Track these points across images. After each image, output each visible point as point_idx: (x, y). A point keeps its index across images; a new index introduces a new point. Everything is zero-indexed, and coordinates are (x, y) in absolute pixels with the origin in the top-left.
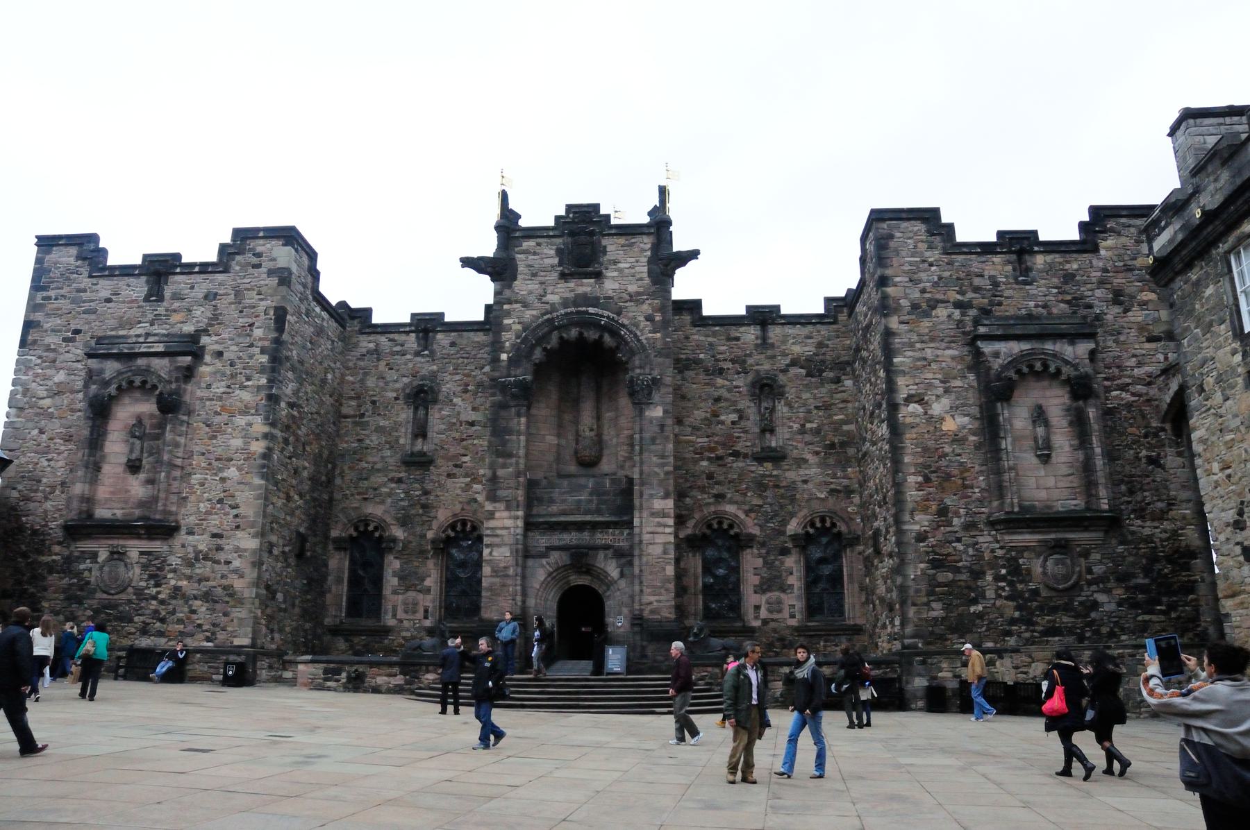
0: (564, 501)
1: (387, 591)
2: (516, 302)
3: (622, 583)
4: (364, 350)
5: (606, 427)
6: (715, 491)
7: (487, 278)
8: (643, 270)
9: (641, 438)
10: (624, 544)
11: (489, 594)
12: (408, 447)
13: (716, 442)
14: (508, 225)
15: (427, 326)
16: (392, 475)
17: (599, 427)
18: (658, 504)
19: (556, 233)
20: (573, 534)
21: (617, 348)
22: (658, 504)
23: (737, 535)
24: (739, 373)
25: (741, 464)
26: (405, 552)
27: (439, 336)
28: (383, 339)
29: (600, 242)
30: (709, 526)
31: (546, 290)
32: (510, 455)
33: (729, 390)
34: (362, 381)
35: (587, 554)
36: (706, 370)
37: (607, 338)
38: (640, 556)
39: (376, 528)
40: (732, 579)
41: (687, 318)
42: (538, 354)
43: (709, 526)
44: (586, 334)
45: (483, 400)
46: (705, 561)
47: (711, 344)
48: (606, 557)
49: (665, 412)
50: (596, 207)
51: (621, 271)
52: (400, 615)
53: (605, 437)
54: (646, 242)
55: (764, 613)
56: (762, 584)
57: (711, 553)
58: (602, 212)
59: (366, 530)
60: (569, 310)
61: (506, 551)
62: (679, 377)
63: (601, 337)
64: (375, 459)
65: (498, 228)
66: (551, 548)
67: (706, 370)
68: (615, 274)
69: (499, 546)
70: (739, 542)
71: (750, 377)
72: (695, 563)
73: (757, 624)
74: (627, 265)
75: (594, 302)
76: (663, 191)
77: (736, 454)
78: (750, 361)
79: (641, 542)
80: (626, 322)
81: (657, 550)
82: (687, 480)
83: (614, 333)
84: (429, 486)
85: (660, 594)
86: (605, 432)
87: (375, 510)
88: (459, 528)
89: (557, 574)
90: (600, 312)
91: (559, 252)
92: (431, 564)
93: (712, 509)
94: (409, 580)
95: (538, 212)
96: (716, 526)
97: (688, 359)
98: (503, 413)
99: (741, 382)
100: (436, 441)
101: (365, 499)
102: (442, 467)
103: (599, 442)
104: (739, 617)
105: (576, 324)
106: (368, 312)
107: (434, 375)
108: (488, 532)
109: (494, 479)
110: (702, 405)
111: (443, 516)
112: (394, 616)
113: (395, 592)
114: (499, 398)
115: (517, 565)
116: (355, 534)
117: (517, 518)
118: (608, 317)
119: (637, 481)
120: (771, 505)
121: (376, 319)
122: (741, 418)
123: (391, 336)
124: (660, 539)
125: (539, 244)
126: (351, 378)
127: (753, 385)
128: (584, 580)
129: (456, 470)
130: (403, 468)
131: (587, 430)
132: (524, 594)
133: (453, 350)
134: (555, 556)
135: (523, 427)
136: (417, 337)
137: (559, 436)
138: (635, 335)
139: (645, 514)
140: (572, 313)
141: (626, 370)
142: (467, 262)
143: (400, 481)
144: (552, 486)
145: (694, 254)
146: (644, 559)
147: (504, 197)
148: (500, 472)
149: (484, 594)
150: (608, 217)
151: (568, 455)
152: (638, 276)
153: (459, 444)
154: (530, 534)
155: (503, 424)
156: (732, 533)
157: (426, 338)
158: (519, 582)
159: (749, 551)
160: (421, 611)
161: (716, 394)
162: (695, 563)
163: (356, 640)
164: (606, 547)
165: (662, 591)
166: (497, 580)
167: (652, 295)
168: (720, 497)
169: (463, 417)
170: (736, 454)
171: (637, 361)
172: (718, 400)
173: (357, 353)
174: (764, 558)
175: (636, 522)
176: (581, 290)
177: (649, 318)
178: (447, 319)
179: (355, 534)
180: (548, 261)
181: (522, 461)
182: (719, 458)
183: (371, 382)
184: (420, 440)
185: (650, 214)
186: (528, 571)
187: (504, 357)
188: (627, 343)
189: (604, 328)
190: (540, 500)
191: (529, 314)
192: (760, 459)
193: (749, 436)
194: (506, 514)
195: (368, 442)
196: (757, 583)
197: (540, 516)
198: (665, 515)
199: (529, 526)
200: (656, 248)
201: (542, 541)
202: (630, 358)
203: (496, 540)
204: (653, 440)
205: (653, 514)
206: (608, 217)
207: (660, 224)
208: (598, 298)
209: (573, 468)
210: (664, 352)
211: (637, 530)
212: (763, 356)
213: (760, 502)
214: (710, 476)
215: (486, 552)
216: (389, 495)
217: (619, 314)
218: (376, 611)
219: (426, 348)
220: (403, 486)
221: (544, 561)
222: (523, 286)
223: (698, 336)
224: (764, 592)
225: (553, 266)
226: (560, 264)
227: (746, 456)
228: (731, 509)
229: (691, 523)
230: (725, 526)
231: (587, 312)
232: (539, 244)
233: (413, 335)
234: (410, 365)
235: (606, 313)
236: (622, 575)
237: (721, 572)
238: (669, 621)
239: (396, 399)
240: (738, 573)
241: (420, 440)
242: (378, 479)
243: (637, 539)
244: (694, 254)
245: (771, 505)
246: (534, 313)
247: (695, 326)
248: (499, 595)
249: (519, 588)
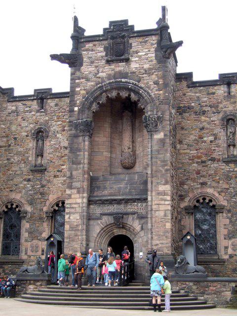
0: (111, 188)
1: (22, 240)
2: (83, 78)
3: (142, 234)
4: (10, 111)
5: (138, 146)
6: (201, 181)
7: (67, 65)
8: (152, 55)
9: (151, 151)
10: (143, 212)
11: (68, 240)
12: (33, 162)
13: (202, 153)
14: (79, 37)
15: (42, 96)
17: (133, 146)
18: (162, 188)
19: (104, 38)
20: (115, 206)
21: (139, 100)
22: (162, 188)
23: (214, 206)
24: (214, 113)
25: (215, 165)
26: (31, 220)
27: (49, 101)
28: (20, 104)
29: (128, 41)
30: (198, 201)
31: (99, 69)
32: (80, 163)
33: (209, 123)
34: (9, 128)
35: (123, 217)
36: (196, 113)
38: (151, 218)
39: (17, 206)
40: (212, 231)
41: (184, 83)
42: (95, 107)
43: (198, 201)
44: (121, 94)
46: (196, 220)
47: (198, 97)
48: (133, 219)
49: (165, 135)
50: (126, 22)
51: (140, 57)
52: (29, 253)
53: (137, 152)
54: (154, 39)
55: (230, 251)
56: (229, 234)
57: (198, 216)
58: (130, 24)
59: (12, 207)
60: (111, 81)
61: (77, 216)
62: (180, 117)
63: (130, 95)
64: (17, 169)
65: (73, 37)
66: (102, 214)
67: (196, 113)
68: (137, 59)
69: (74, 213)
70: (214, 210)
71: (221, 115)
72: (189, 222)
73: (226, 257)
74: (144, 53)
75: (125, 75)
76: (164, 9)
77: (213, 160)
78: (221, 106)
79: (152, 210)
80: (143, 86)
81: (162, 214)
82: (184, 175)
83: (137, 93)
84: (44, 183)
85: (163, 240)
86: (137, 149)
87: (16, 197)
88: (60, 205)
89: (106, 229)
90: (128, 81)
91: (106, 49)
92: (45, 224)
93: (200, 191)
94: (34, 234)
95: (94, 27)
96: (201, 201)
97: (185, 107)
98: (75, 140)
99: (216, 118)
100: (48, 158)
101: (11, 191)
102: (51, 171)
103: (134, 154)
104: (216, 253)
105: (115, 89)
106: (11, 90)
107: (47, 122)
108: (68, 206)
109: (71, 177)
110: (193, 132)
111: (52, 198)
112: (26, 254)
113: (26, 241)
114: (73, 132)
115: (83, 224)
116: (6, 210)
117: (83, 198)
118: (133, 84)
119: (149, 175)
120: (234, 188)
121: (16, 94)
122: (215, 139)
123: (24, 102)
124: (162, 208)
125: (95, 45)
126: (3, 126)
127: (222, 119)
128: (122, 232)
129: (58, 174)
131: (126, 148)
132: (88, 240)
133: (56, 108)
134: (105, 218)
135: (86, 148)
136: (37, 103)
137: (111, 152)
138: (148, 93)
139: (154, 193)
140: (113, 82)
141: (144, 113)
142: (54, 57)
143: (29, 180)
144: (105, 180)
146: (154, 220)
147: (76, 20)
148: (74, 173)
150: (132, 27)
151: (117, 163)
152: (149, 59)
153: (60, 159)
154: (92, 206)
155: (76, 146)
156: (211, 204)
157: (42, 103)
158: (84, 233)
159: (221, 214)
160: (40, 251)
161: (201, 126)
162: (189, 222)
163: (6, 267)
164: (133, 213)
165: (164, 237)
166: (73, 232)
167: (158, 70)
168: (203, 184)
169: (62, 144)
170: (213, 160)
171: (149, 108)
172: (203, 129)
173: (6, 112)
174: (230, 219)
175: (149, 198)
176: (117, 69)
177: (156, 83)
178: (53, 92)
179: (6, 210)
180: (99, 54)
181: (86, 166)
182: (203, 162)
183: (14, 128)
184: (40, 158)
185: (157, 23)
186: (91, 227)
187: (76, 109)
188: (143, 98)
189: (130, 90)
190: (99, 188)
191: (90, 84)
192: (227, 162)
193: (221, 149)
194: (78, 196)
195: (12, 160)
196: (226, 233)
197: (97, 196)
198: (165, 194)
199: (90, 202)
200: (159, 43)
201: (97, 210)
202: (145, 106)
203: (72, 210)
204: (158, 151)
205: (159, 194)
206: (132, 27)
207: (162, 29)
208: (127, 73)
209: (120, 170)
210: (166, 101)
211: (149, 203)
212: (228, 103)
213: (228, 187)
214: (198, 173)
215: (67, 217)
216: (24, 188)
217: (139, 82)
218: (17, 251)
219: (42, 108)
220: (31, 183)
221: (99, 222)
222: (86, 69)
223: (191, 93)
224: (230, 239)
225: (102, 57)
226: (106, 55)
227: (219, 160)
228: (210, 191)
229: (187, 199)
230: (207, 201)
231: (121, 82)
232: (95, 45)
233: (36, 101)
234: (34, 118)
235: (131, 81)
236: (142, 229)
237: (205, 227)
238: (167, 255)
239: (27, 136)
240: (215, 227)
241: (40, 158)
242: (17, 180)
243: (149, 209)
245: (234, 188)
246: (92, 83)
247: (189, 87)
248: (73, 241)
249: (84, 237)
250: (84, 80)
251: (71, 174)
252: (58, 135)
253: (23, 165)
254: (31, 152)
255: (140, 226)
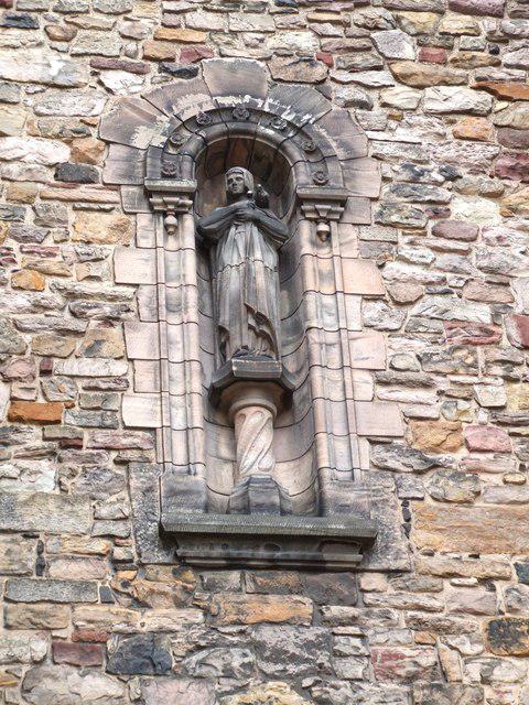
16: (93, 613)
100: (387, 421)
130: (166, 581)
239: (72, 175)
252: (460, 207)
253: (46, 475)
254: (140, 343)
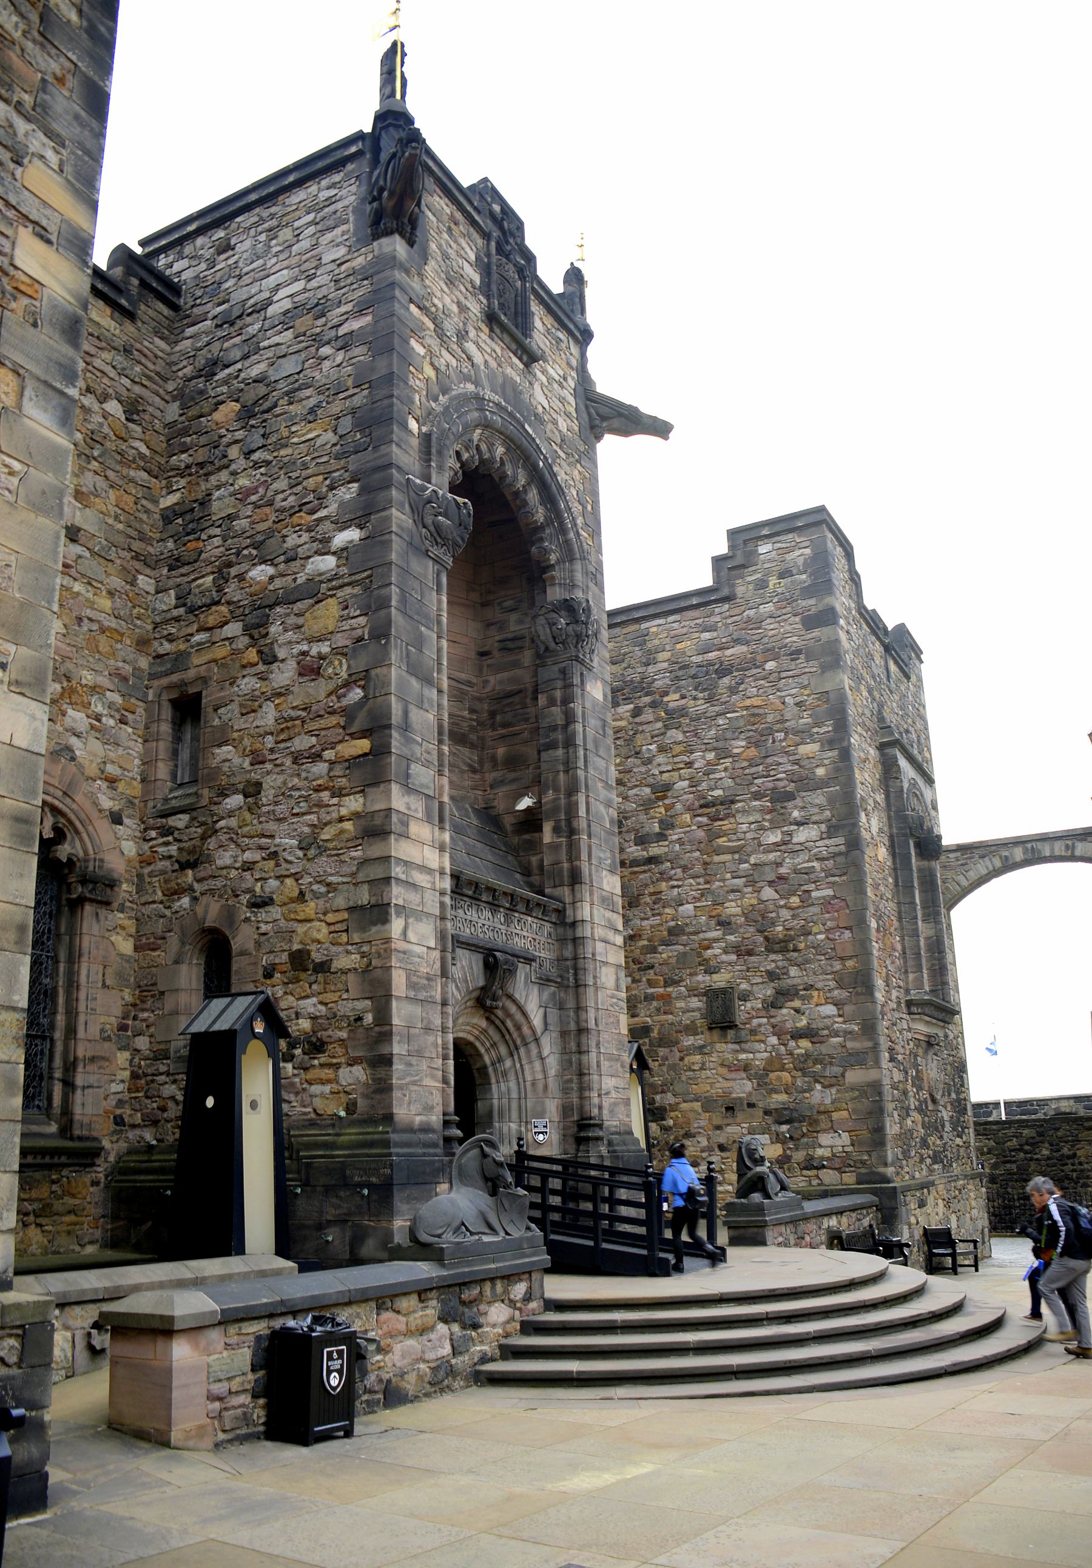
37: (533, 496)
45: (101, 483)
68: (544, 379)
145: (660, 429)
148: (415, 715)
149: (398, 1048)
215: (396, 925)
244: (660, 429)
248: (419, 1054)
250: (432, 326)
251: (406, 713)
255: (542, 1010)
